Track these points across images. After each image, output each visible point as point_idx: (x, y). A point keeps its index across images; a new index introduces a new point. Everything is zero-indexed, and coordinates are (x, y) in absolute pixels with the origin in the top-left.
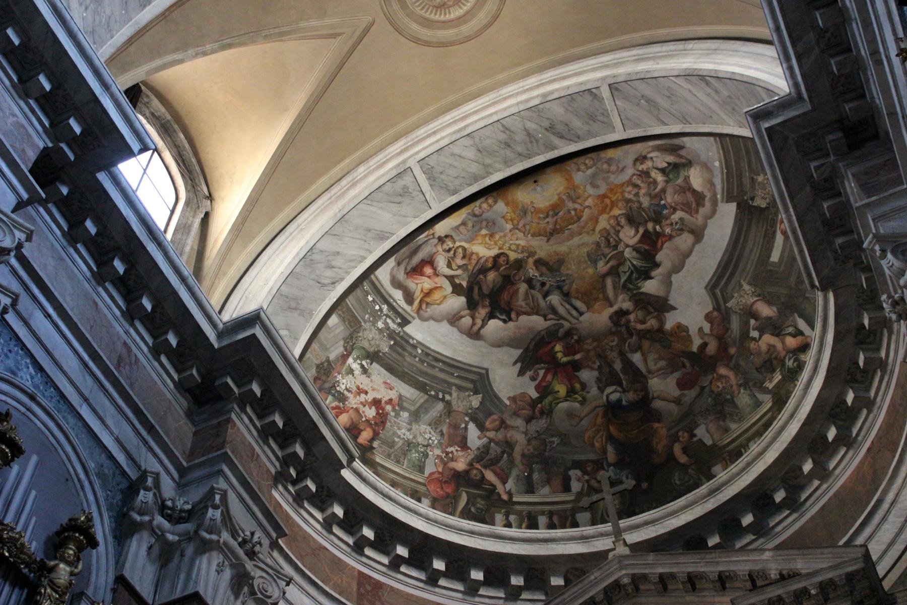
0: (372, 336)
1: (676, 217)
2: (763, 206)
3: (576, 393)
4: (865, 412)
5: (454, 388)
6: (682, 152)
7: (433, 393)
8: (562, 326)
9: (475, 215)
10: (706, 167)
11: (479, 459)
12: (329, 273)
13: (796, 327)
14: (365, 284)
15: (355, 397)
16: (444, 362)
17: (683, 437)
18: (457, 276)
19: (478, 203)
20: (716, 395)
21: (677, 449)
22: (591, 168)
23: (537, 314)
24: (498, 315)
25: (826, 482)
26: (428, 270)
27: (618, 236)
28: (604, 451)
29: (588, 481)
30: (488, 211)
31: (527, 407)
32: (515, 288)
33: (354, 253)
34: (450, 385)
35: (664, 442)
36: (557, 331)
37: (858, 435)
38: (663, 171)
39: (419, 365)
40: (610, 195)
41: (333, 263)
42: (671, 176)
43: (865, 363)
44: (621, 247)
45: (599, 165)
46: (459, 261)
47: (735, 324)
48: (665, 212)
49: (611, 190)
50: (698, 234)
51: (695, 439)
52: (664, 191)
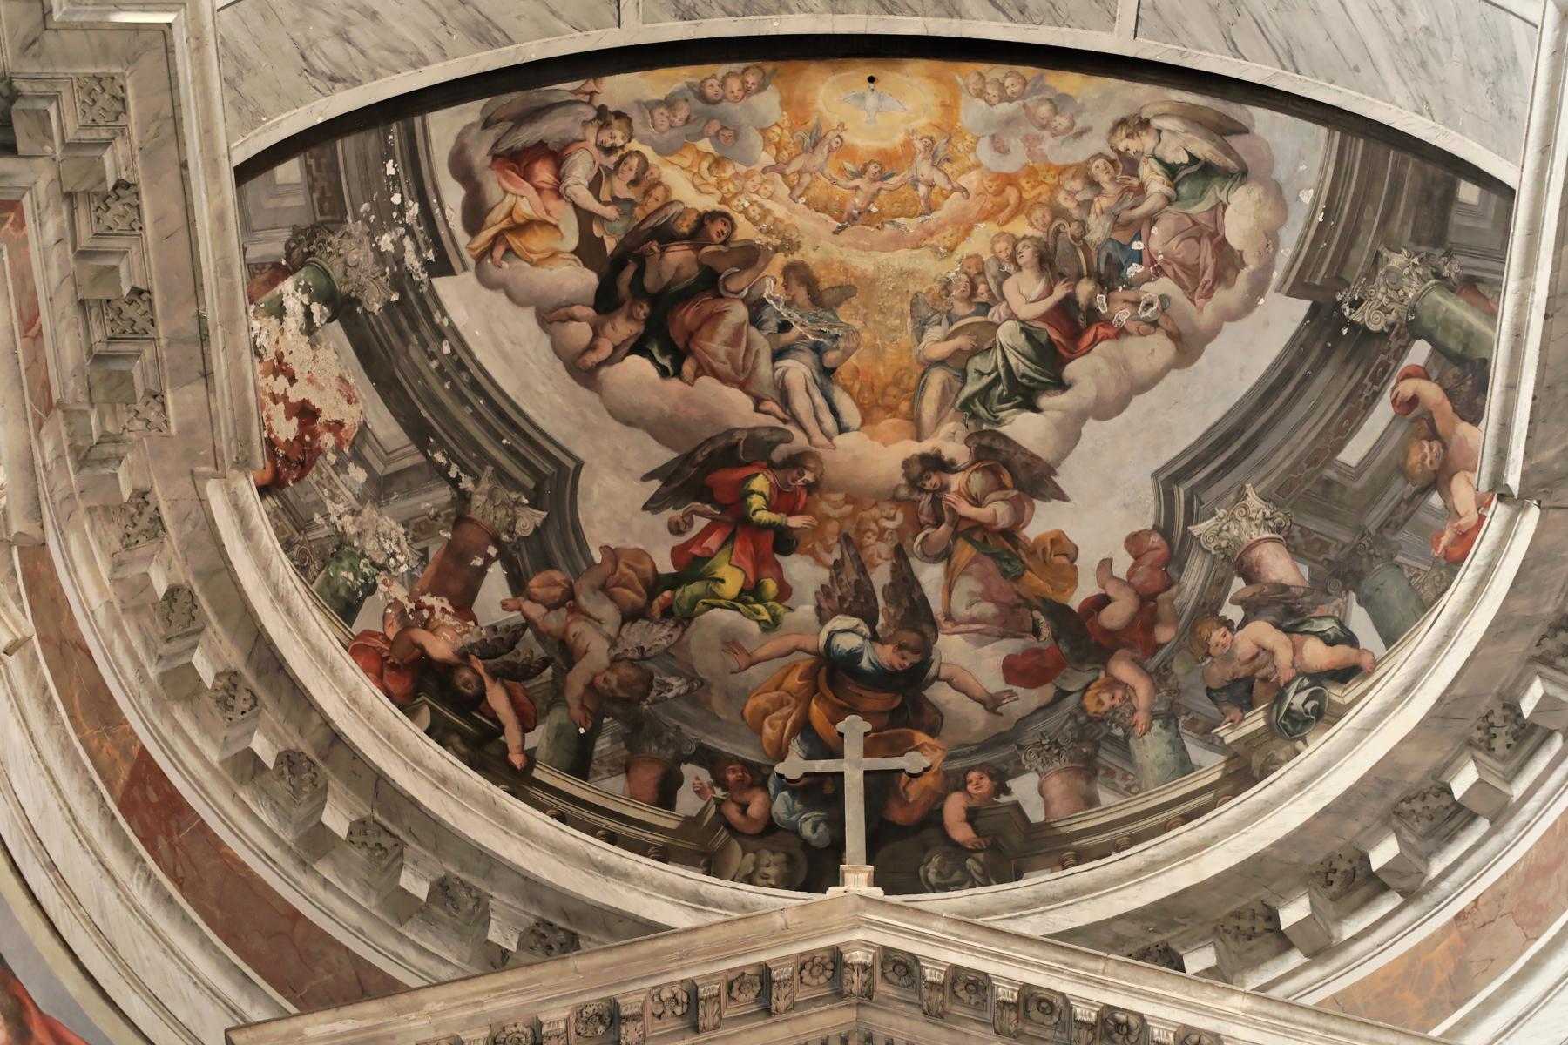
0: (355, 254)
1: (1152, 290)
2: (1374, 328)
3: (761, 600)
4: (1483, 825)
5: (490, 468)
6: (1236, 142)
7: (440, 458)
8: (788, 438)
9: (702, 97)
10: (1278, 196)
12: (334, 48)
13: (1341, 624)
14: (394, 128)
15: (265, 374)
16: (490, 402)
17: (978, 786)
18: (602, 219)
19: (722, 69)
20: (1090, 719)
21: (954, 807)
22: (1010, 100)
23: (742, 387)
24: (655, 351)
25: (1321, 964)
26: (544, 173)
27: (1000, 285)
29: (719, 803)
30: (737, 100)
31: (640, 587)
32: (723, 305)
33: (409, 36)
34: (484, 458)
35: (929, 780)
36: (773, 445)
37: (1443, 876)
38: (1171, 170)
39: (433, 380)
40: (1023, 183)
41: (354, 33)
42: (1183, 190)
43: (1539, 709)
44: (995, 314)
45: (1030, 102)
46: (621, 188)
47: (1193, 578)
48: (1134, 270)
49: (1031, 172)
51: (1004, 799)
52: (1152, 219)
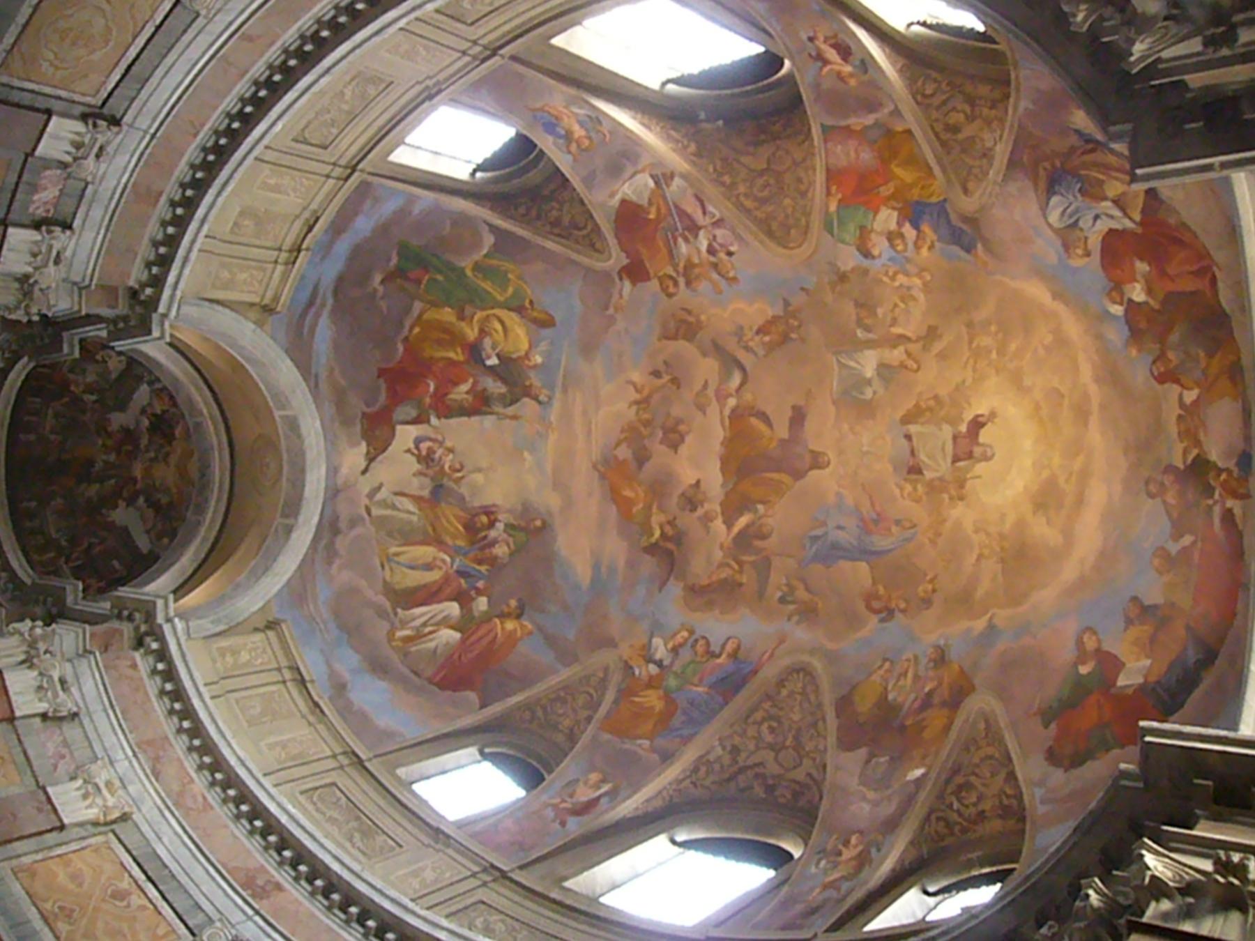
21: (54, 488)
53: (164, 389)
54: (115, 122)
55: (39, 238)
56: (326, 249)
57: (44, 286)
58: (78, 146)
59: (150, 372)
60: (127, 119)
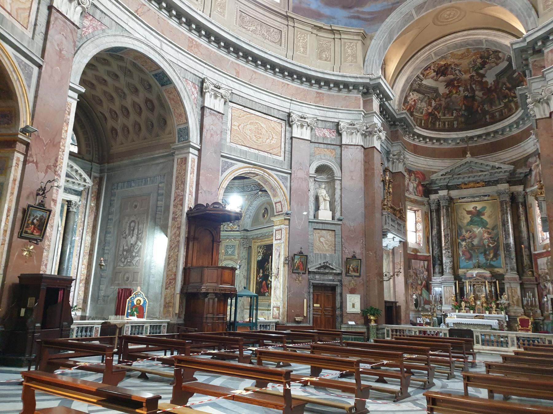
11: (434, 109)
21: (479, 109)
28: (462, 107)
47: (500, 85)
50: (497, 64)
53: (422, 73)
54: (289, 115)
55: (345, 133)
56: (330, 18)
57: (365, 128)
58: (302, 126)
59: (415, 80)
60: (287, 111)
